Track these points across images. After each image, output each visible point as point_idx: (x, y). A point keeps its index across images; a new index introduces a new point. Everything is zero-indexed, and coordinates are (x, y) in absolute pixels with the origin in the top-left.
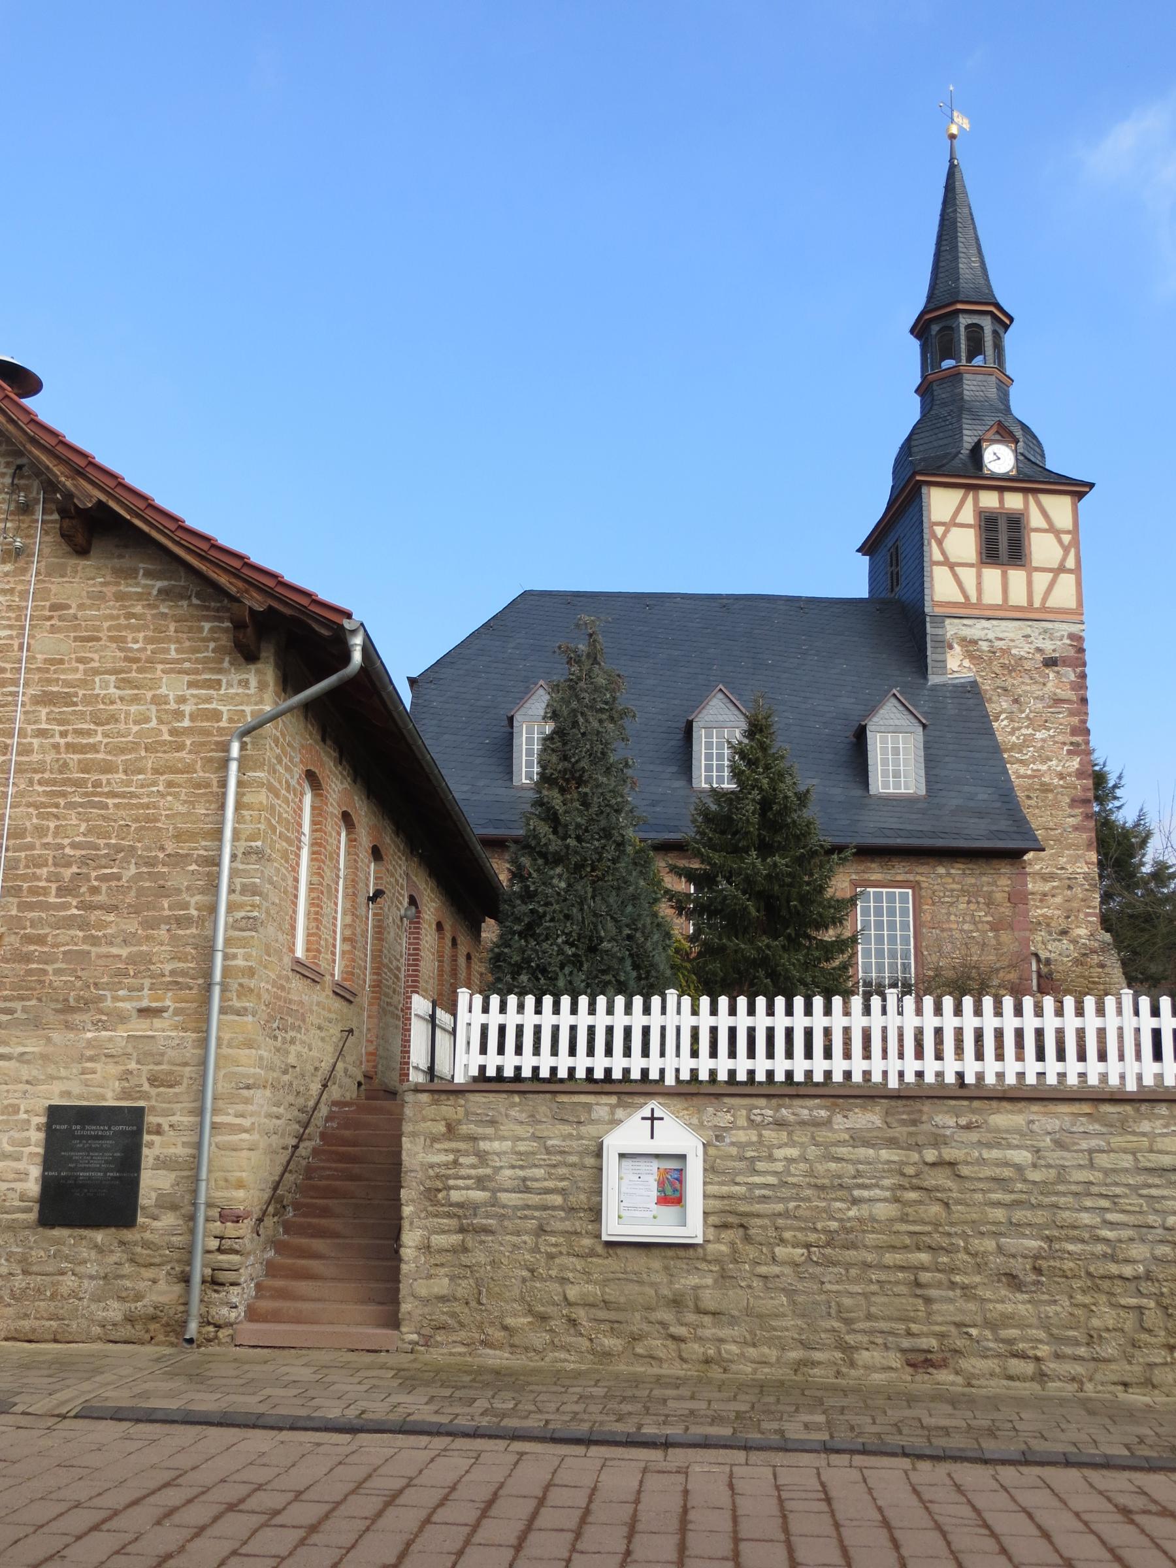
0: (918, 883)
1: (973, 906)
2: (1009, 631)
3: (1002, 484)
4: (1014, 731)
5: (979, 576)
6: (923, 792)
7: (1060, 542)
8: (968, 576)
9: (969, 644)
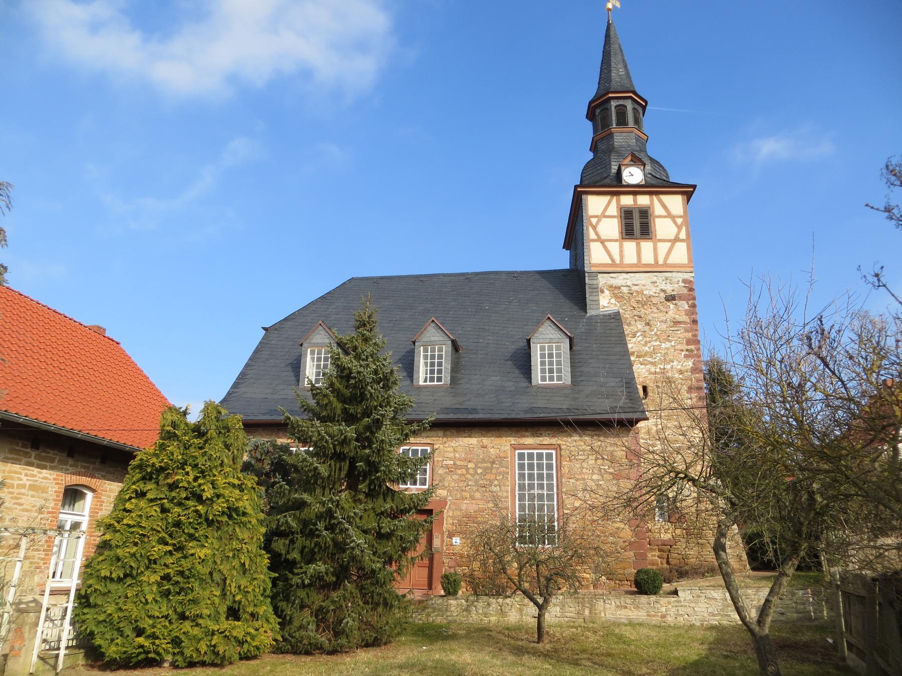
0: (559, 446)
1: (599, 462)
2: (642, 279)
3: (635, 190)
4: (646, 343)
5: (621, 246)
6: (567, 379)
7: (675, 223)
8: (614, 247)
9: (615, 290)
